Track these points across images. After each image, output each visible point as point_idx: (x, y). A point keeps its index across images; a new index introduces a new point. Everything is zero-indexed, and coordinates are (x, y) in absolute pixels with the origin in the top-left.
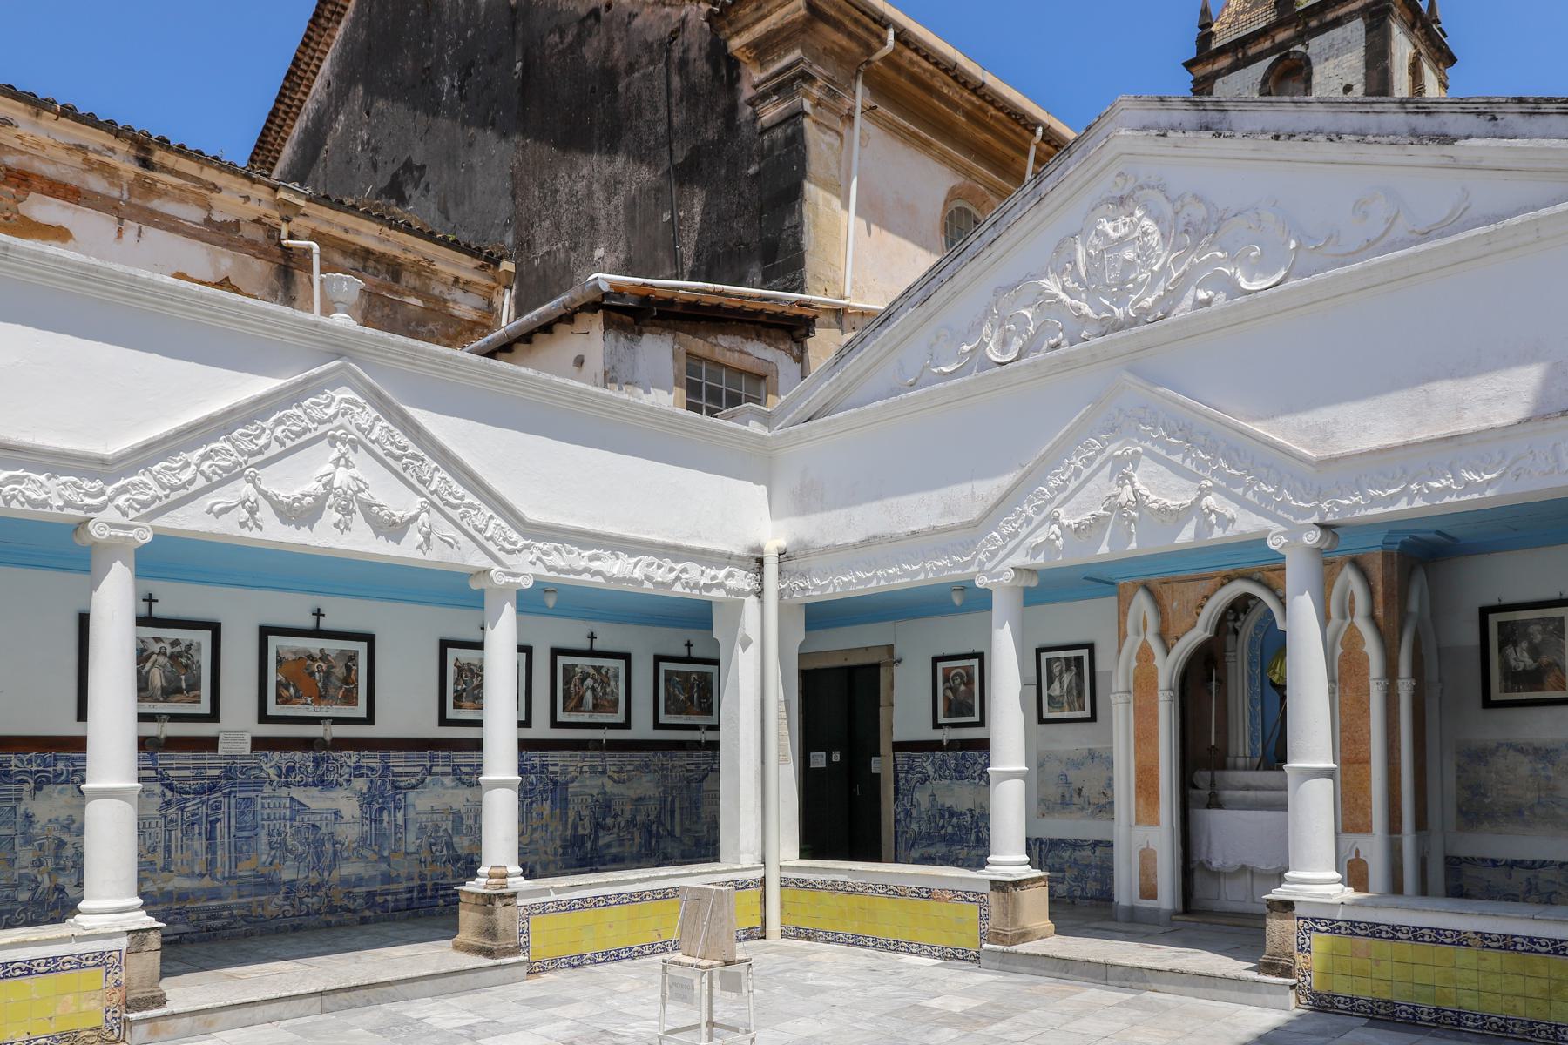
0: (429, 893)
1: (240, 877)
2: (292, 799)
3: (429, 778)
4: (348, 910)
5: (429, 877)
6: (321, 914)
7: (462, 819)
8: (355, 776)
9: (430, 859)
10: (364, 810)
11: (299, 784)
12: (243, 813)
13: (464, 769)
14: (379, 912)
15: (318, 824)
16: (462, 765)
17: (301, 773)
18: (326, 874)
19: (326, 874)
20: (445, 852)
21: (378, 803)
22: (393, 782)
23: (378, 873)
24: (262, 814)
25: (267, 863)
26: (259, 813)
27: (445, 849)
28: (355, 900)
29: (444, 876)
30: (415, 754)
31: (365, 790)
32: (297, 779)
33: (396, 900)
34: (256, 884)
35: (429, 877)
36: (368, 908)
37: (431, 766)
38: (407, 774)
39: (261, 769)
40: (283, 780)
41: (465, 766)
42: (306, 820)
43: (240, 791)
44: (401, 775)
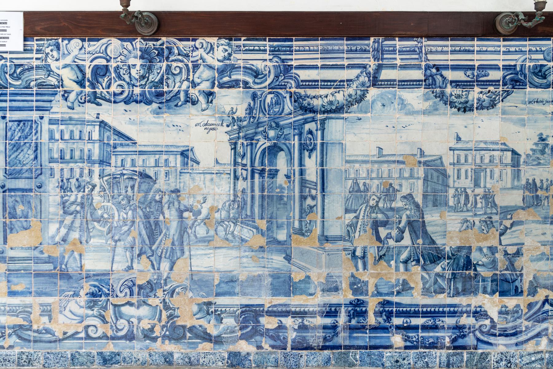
0: (372, 320)
1: (12, 259)
2: (103, 125)
3: (373, 92)
4: (207, 337)
5: (371, 289)
6: (154, 339)
7: (444, 175)
8: (221, 86)
9: (372, 252)
10: (240, 150)
11: (114, 99)
12: (17, 147)
13: (450, 75)
14: (266, 346)
15: (151, 173)
16: (446, 67)
17: (119, 77)
18: (165, 265)
19: (165, 265)
20: (407, 241)
21: (266, 137)
22: (297, 99)
23: (266, 272)
24: (50, 150)
25: (57, 239)
26: (45, 149)
27: (407, 235)
28: (220, 320)
29: (405, 288)
30: (344, 44)
31: (241, 112)
32: (114, 88)
33: (303, 328)
34: (37, 275)
35: (371, 289)
36: (246, 337)
37: (380, 68)
38: (327, 84)
39: (49, 72)
40: (88, 90)
41: (455, 68)
42: (128, 164)
43: (12, 109)
44: (313, 84)
